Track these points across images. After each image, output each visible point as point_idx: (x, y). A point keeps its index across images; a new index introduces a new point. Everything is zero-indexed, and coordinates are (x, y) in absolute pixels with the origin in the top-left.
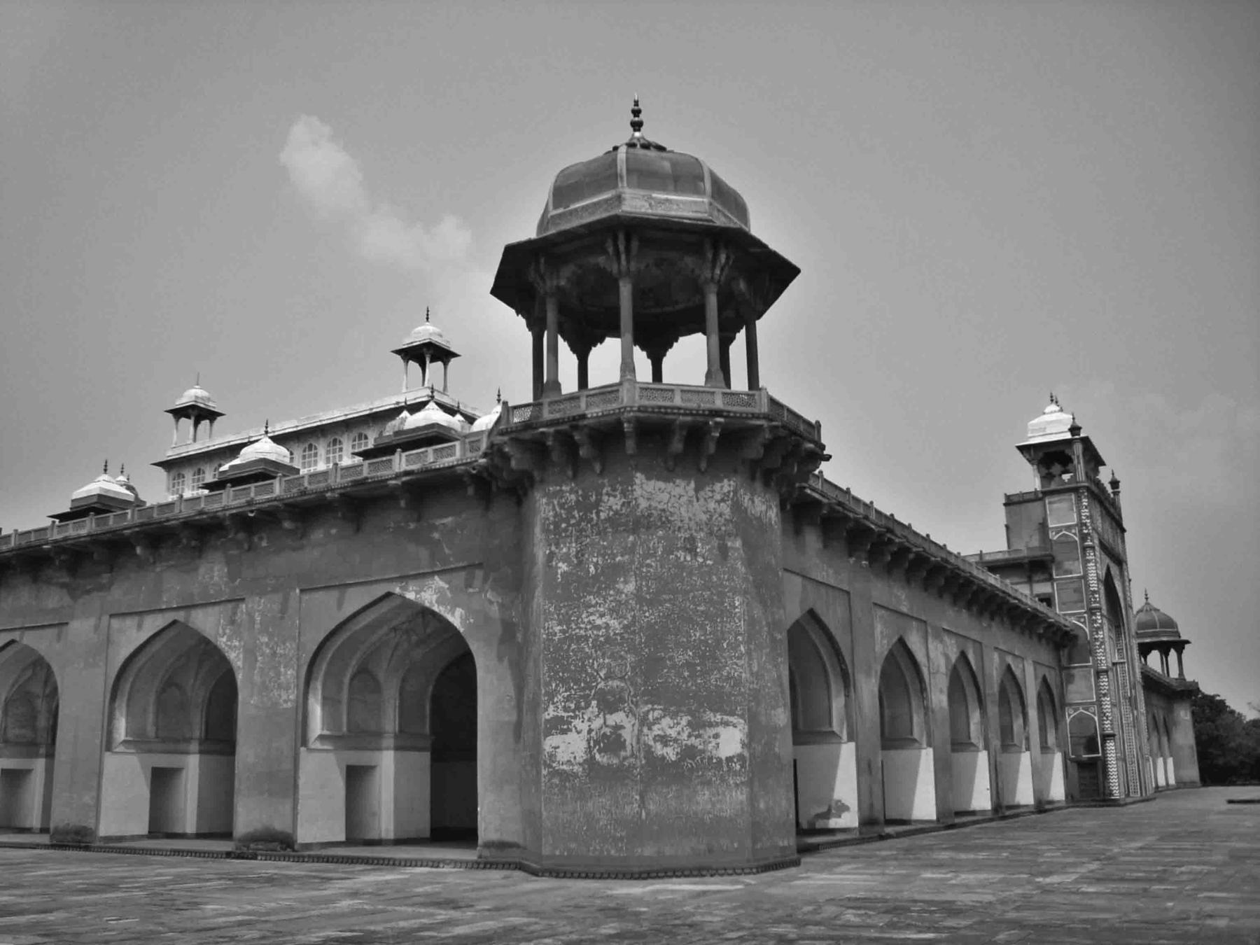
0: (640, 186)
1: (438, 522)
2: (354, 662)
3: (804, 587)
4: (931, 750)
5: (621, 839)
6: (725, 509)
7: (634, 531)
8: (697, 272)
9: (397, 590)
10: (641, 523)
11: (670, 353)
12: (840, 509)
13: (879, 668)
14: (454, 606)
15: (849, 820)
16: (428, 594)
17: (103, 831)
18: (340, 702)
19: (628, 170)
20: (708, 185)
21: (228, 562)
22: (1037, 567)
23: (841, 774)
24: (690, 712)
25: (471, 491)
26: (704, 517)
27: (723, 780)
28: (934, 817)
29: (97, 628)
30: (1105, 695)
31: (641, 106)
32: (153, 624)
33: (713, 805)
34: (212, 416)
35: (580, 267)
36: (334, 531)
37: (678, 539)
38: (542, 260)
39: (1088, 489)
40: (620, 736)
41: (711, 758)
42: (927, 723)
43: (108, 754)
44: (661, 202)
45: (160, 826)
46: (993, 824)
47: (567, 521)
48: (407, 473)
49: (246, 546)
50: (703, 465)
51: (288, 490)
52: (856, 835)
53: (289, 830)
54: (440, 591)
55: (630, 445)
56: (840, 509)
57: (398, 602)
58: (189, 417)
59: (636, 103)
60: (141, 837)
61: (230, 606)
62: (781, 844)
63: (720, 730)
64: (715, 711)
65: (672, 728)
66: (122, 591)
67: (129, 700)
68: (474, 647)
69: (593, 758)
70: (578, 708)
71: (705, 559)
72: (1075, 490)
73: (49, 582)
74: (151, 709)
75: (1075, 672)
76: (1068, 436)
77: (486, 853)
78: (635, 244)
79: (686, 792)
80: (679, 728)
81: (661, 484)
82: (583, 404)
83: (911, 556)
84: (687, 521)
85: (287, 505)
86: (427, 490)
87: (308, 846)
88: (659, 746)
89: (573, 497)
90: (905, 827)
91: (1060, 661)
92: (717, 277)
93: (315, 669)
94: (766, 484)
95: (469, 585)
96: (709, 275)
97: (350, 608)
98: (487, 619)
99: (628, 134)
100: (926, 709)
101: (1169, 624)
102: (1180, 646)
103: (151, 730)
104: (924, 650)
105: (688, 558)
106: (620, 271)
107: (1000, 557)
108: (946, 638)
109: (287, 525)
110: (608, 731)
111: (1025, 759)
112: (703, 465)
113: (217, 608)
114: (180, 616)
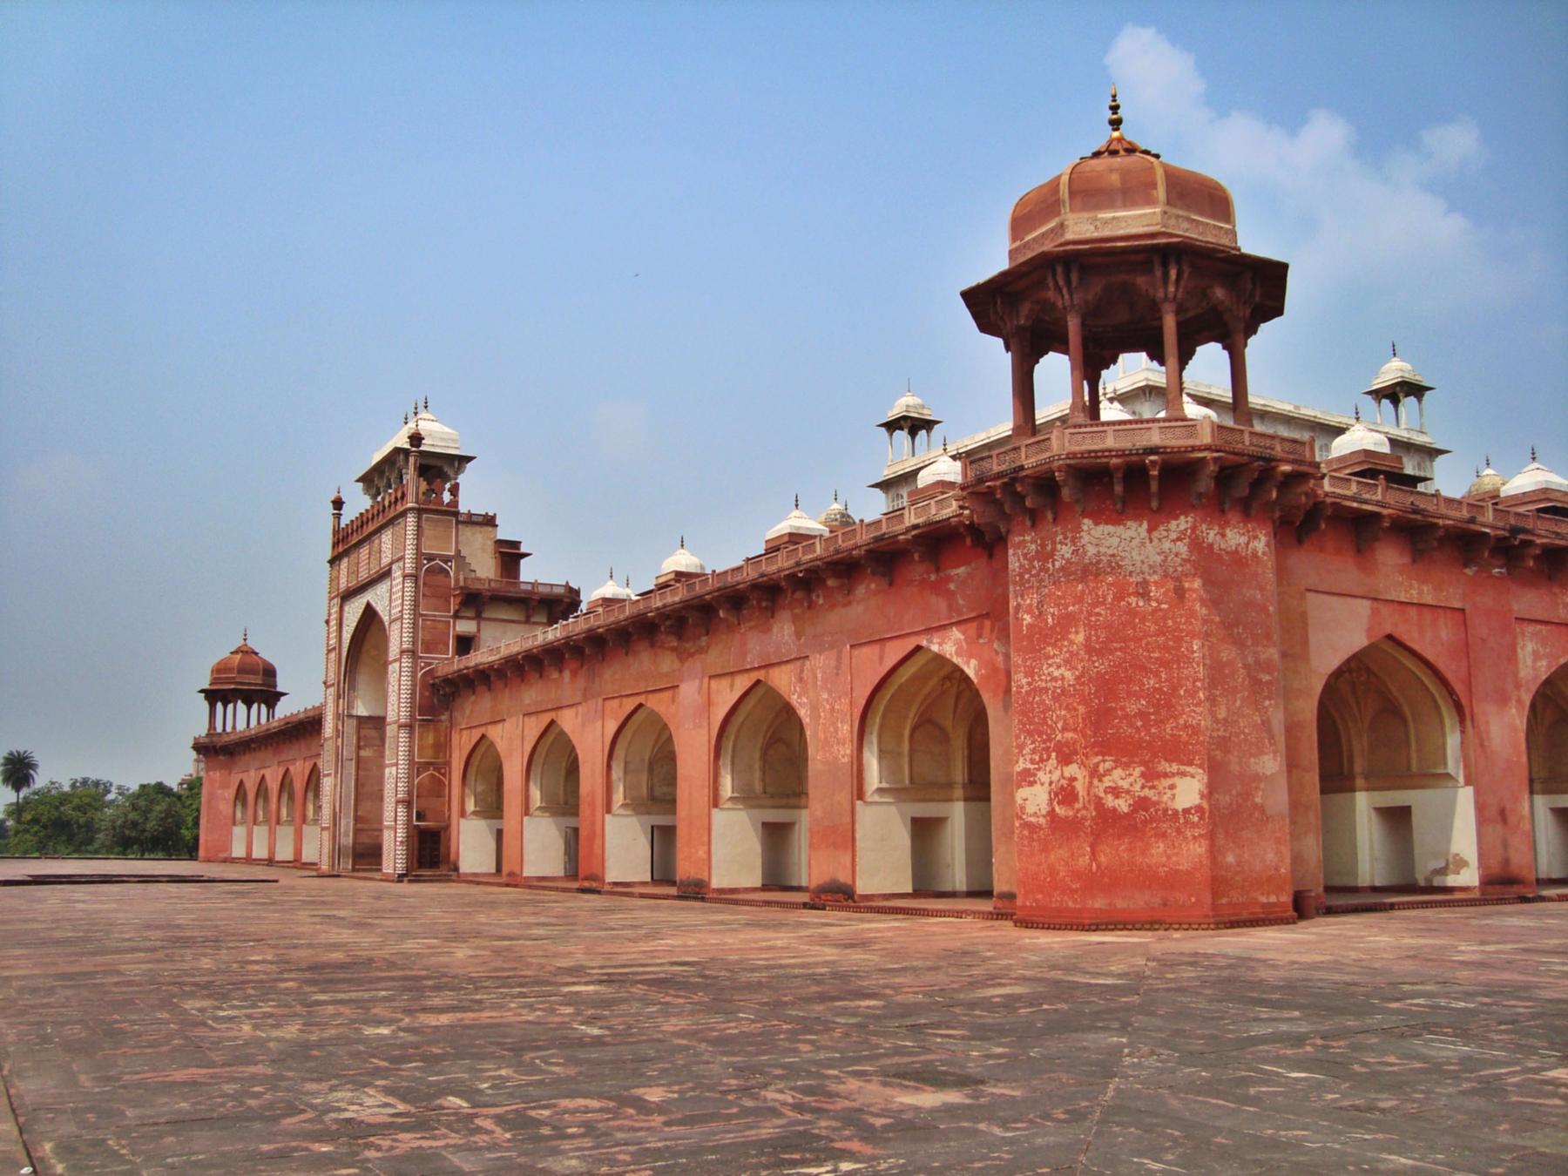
0: (1086, 207)
2: (911, 715)
3: (1375, 612)
5: (1076, 891)
6: (1182, 548)
7: (1083, 579)
8: (1151, 292)
9: (924, 643)
10: (1089, 571)
11: (1247, 351)
12: (1419, 517)
13: (1527, 699)
14: (970, 656)
15: (1469, 877)
16: (949, 645)
17: (715, 884)
18: (900, 754)
19: (1072, 194)
20: (1161, 192)
21: (796, 620)
24: (1143, 763)
25: (968, 541)
26: (1159, 559)
27: (1179, 831)
29: (700, 689)
32: (742, 683)
33: (1169, 857)
34: (928, 425)
36: (873, 586)
37: (1130, 584)
40: (1073, 788)
43: (715, 811)
44: (1106, 222)
48: (915, 527)
50: (1154, 504)
51: (826, 549)
52: (1476, 895)
54: (957, 643)
56: (1419, 517)
61: (799, 663)
62: (1264, 899)
63: (1177, 780)
65: (1128, 778)
66: (718, 654)
67: (733, 758)
68: (987, 698)
70: (1042, 760)
71: (1160, 603)
73: (662, 647)
74: (757, 766)
77: (1000, 905)
78: (1074, 277)
79: (1139, 844)
80: (1131, 779)
81: (1110, 528)
86: (936, 542)
95: (980, 636)
97: (890, 662)
98: (995, 669)
103: (758, 787)
109: (830, 583)
110: (1064, 782)
112: (1154, 504)
113: (789, 667)
114: (760, 675)
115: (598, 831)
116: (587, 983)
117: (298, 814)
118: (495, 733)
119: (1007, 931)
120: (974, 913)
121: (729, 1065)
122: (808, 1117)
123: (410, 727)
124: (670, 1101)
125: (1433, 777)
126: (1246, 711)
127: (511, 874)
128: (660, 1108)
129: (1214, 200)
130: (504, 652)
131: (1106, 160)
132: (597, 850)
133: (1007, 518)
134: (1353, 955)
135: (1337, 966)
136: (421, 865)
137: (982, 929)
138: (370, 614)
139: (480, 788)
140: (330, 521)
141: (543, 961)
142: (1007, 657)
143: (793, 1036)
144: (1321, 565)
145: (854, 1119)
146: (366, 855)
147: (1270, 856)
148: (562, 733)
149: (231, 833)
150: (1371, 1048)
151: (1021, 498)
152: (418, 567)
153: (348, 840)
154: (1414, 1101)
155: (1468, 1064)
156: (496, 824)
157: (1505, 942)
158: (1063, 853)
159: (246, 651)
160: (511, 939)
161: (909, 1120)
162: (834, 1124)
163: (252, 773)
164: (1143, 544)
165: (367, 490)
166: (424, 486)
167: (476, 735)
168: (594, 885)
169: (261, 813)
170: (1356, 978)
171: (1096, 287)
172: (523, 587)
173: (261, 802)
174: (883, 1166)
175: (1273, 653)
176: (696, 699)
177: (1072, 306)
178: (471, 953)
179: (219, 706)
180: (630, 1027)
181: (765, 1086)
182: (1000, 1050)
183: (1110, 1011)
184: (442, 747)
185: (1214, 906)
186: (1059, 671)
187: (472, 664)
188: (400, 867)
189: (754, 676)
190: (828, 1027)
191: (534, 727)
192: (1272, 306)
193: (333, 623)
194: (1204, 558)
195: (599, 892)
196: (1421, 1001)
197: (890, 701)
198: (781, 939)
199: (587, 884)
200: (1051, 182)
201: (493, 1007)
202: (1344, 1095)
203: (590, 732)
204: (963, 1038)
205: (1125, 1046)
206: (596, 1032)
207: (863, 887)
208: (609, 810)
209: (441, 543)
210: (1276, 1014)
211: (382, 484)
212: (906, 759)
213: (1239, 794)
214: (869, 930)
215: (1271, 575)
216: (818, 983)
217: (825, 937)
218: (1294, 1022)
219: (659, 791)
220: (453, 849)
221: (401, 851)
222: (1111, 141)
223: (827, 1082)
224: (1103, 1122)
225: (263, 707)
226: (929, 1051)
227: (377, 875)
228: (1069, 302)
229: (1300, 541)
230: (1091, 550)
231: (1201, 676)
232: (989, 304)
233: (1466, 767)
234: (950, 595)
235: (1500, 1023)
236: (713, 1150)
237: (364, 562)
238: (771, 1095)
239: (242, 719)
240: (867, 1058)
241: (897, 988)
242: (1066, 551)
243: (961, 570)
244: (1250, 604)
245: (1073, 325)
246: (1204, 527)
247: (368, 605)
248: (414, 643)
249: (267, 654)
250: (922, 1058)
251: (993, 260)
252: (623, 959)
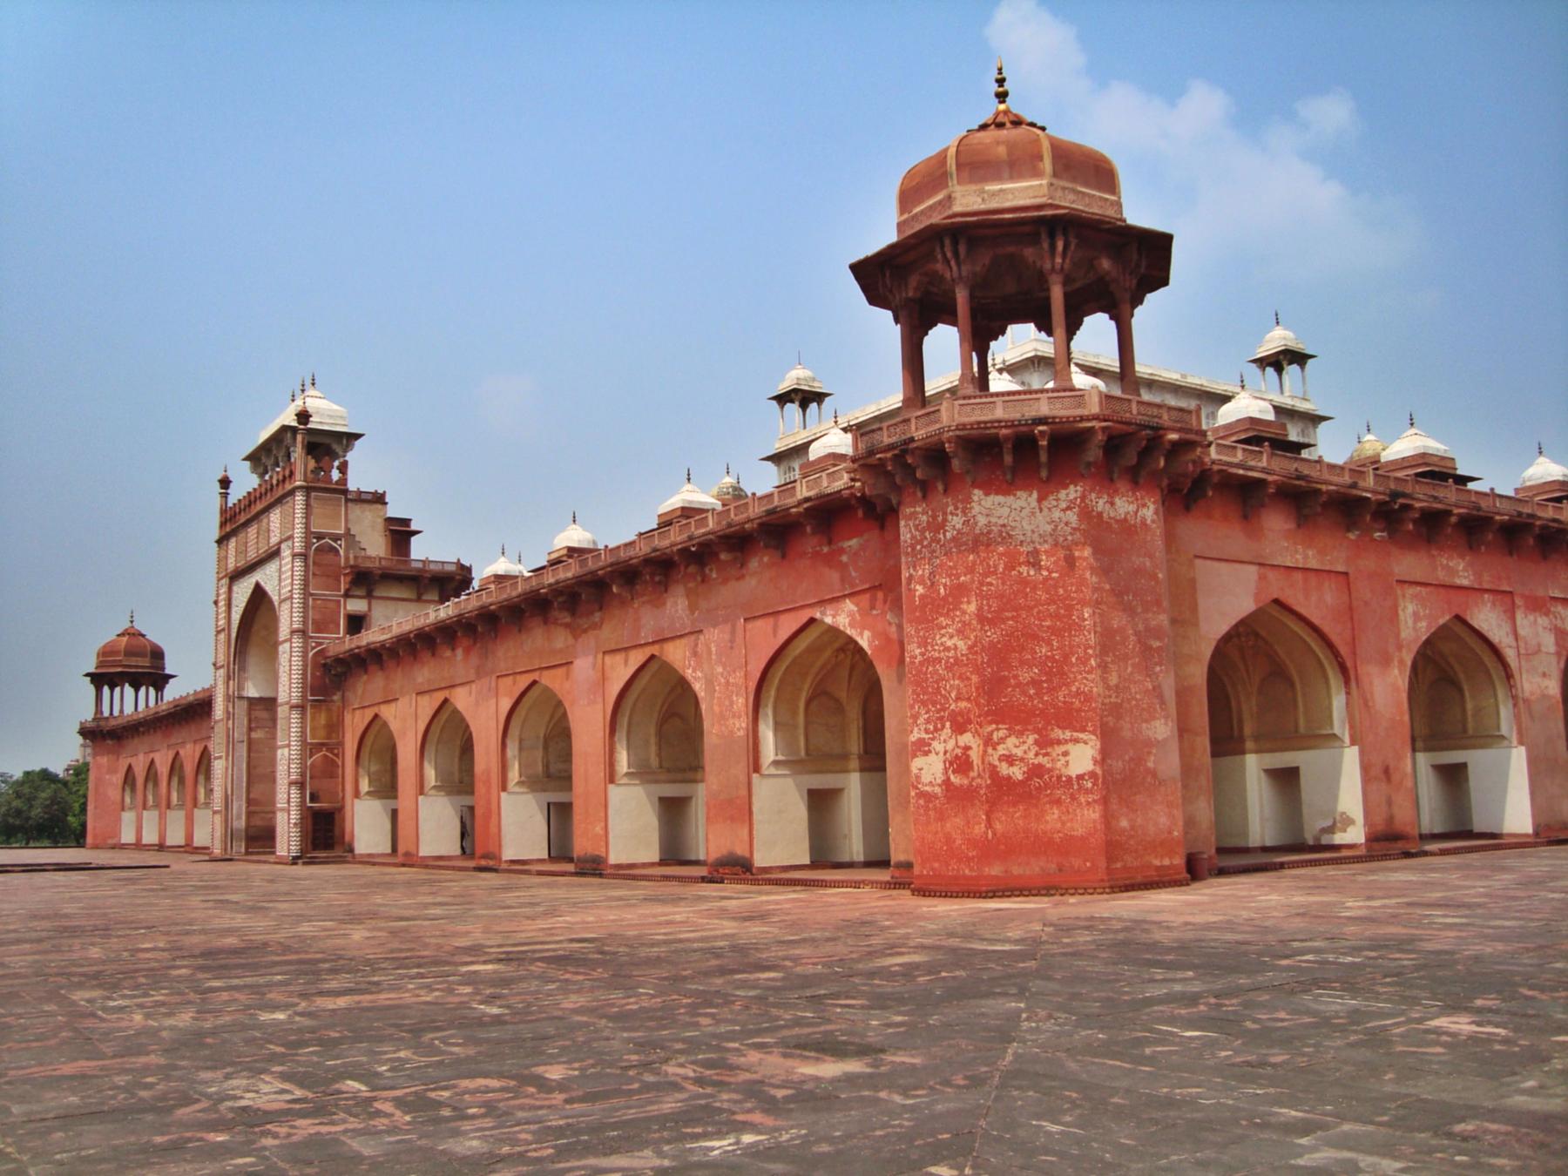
0: (972, 181)
1: (846, 544)
2: (806, 686)
3: (1262, 578)
4: (1522, 749)
6: (1072, 517)
7: (974, 550)
8: (1039, 264)
9: (818, 616)
10: (980, 542)
11: (1134, 321)
14: (863, 628)
15: (1355, 835)
16: (842, 617)
17: (613, 859)
18: (795, 727)
19: (958, 165)
20: (1047, 164)
24: (1037, 731)
25: (860, 513)
26: (1049, 528)
27: (1073, 798)
28: (1530, 830)
29: (594, 666)
31: (1004, 74)
32: (637, 658)
33: (1063, 823)
34: (819, 397)
36: (766, 559)
37: (1021, 554)
42: (1517, 717)
43: (611, 787)
44: (994, 194)
47: (920, 542)
48: (807, 500)
50: (1044, 474)
51: (719, 523)
52: (1362, 852)
53: (747, 855)
54: (851, 614)
55: (956, 464)
58: (792, 401)
60: (652, 865)
61: (693, 638)
62: (1157, 862)
63: (1070, 747)
64: (1063, 728)
65: (1021, 746)
66: (611, 630)
67: (629, 732)
70: (936, 730)
73: (555, 622)
74: (653, 740)
78: (962, 249)
79: (1034, 811)
80: (1025, 747)
81: (1000, 499)
83: (1453, 519)
85: (720, 537)
86: (828, 515)
89: (925, 518)
90: (1494, 841)
93: (764, 694)
94: (1135, 483)
95: (873, 607)
97: (784, 635)
98: (888, 640)
100: (1514, 697)
103: (654, 762)
104: (1506, 627)
108: (1559, 608)
109: (723, 556)
110: (958, 751)
112: (1044, 474)
113: (684, 641)
114: (655, 650)
115: (494, 806)
116: (485, 962)
117: (189, 798)
118: (387, 712)
119: (905, 900)
121: (629, 1040)
122: (709, 1090)
123: (301, 708)
124: (569, 1079)
125: (1321, 738)
126: (1137, 677)
127: (407, 854)
128: (561, 1086)
129: (1100, 172)
130: (396, 631)
131: (992, 133)
132: (493, 830)
133: (899, 489)
134: (1245, 914)
135: (1230, 926)
136: (315, 847)
137: (879, 899)
138: (259, 594)
139: (374, 768)
140: (218, 500)
141: (440, 941)
142: (900, 627)
143: (693, 1010)
144: (1209, 532)
145: (756, 1092)
146: (260, 838)
147: (1163, 821)
148: (456, 712)
149: (119, 820)
150: (1262, 1005)
151: (910, 470)
152: (308, 545)
153: (240, 824)
154: (1304, 1055)
155: (1356, 1016)
156: (391, 804)
157: (1390, 897)
158: (959, 821)
159: (133, 634)
160: (407, 919)
161: (811, 1092)
162: (735, 1096)
163: (141, 757)
164: (1033, 513)
165: (254, 469)
166: (312, 464)
167: (369, 714)
168: (491, 863)
169: (150, 798)
170: (1248, 937)
171: (985, 258)
172: (414, 565)
173: (150, 786)
174: (785, 1137)
175: (1163, 619)
176: (591, 675)
177: (960, 277)
178: (368, 934)
179: (106, 690)
180: (529, 1005)
181: (666, 1061)
182: (899, 1019)
183: (1010, 976)
184: (335, 727)
185: (1109, 870)
186: (951, 641)
187: (364, 643)
188: (295, 849)
189: (648, 651)
190: (728, 1001)
191: (428, 706)
192: (1159, 278)
193: (222, 603)
194: (1095, 527)
195: (496, 871)
196: (1310, 957)
197: (785, 673)
198: (680, 913)
199: (483, 863)
200: (939, 154)
201: (392, 989)
202: (1237, 1052)
203: (484, 708)
204: (862, 1007)
205: (1022, 1011)
206: (495, 1011)
207: (760, 860)
208: (504, 788)
209: (331, 522)
210: (1170, 975)
211: (270, 462)
212: (801, 731)
213: (1131, 759)
214: (768, 902)
215: (1159, 543)
216: (718, 956)
217: (723, 910)
218: (1188, 982)
219: (553, 769)
220: (348, 830)
221: (295, 834)
222: (997, 114)
223: (728, 1055)
224: (1002, 1086)
225: (151, 690)
226: (829, 1021)
227: (271, 858)
228: (957, 274)
229: (1187, 509)
230: (982, 521)
231: (1092, 643)
232: (878, 277)
233: (1352, 727)
234: (843, 567)
235: (1385, 976)
236: (614, 1126)
237: (253, 542)
238: (671, 1069)
239: (129, 703)
240: (767, 1030)
241: (796, 960)
242: (956, 521)
243: (854, 542)
244: (1139, 572)
245: (961, 296)
246: (1093, 496)
247: (258, 586)
248: (305, 622)
249: (155, 636)
250: (822, 1028)
251: (881, 233)
252: (522, 937)
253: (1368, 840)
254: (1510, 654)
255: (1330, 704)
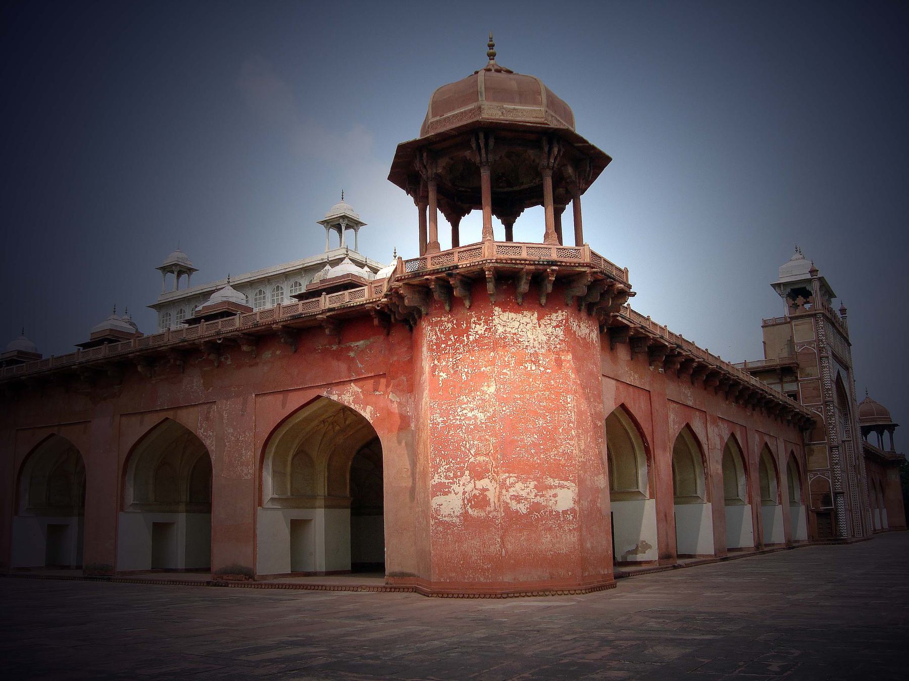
1: (353, 344)
3: (617, 388)
5: (488, 569)
6: (560, 332)
7: (494, 349)
8: (537, 161)
9: (325, 394)
10: (499, 343)
15: (652, 554)
16: (348, 396)
22: (786, 372)
23: (645, 522)
25: (376, 322)
26: (545, 338)
27: (560, 527)
30: (836, 464)
31: (494, 42)
32: (151, 421)
33: (554, 545)
34: (190, 271)
35: (452, 159)
36: (278, 352)
38: (425, 155)
39: (823, 315)
41: (551, 512)
42: (707, 485)
44: (510, 111)
45: (159, 565)
46: (754, 557)
48: (330, 310)
49: (216, 364)
50: (543, 301)
52: (657, 566)
55: (490, 287)
57: (325, 402)
58: (173, 273)
59: (491, 39)
61: (205, 407)
63: (558, 491)
69: (467, 512)
70: (455, 476)
71: (546, 369)
72: (814, 315)
75: (814, 447)
76: (809, 276)
77: (391, 581)
78: (491, 143)
80: (528, 490)
81: (512, 315)
82: (456, 259)
83: (695, 365)
84: (532, 341)
87: (264, 577)
88: (514, 503)
89: (450, 325)
91: (803, 440)
92: (551, 165)
93: (267, 451)
94: (589, 314)
95: (376, 390)
96: (545, 164)
98: (390, 413)
99: (485, 62)
100: (706, 474)
101: (884, 413)
102: (891, 428)
105: (534, 368)
106: (481, 163)
107: (759, 365)
108: (720, 424)
109: (245, 348)
110: (477, 492)
111: (778, 509)
112: (543, 301)
113: (196, 409)
114: (170, 415)
120: (367, 587)
177: (487, 162)
189: (163, 415)
207: (260, 570)
212: (289, 478)
243: (361, 343)
253: (659, 558)
254: (705, 447)
255: (637, 473)
